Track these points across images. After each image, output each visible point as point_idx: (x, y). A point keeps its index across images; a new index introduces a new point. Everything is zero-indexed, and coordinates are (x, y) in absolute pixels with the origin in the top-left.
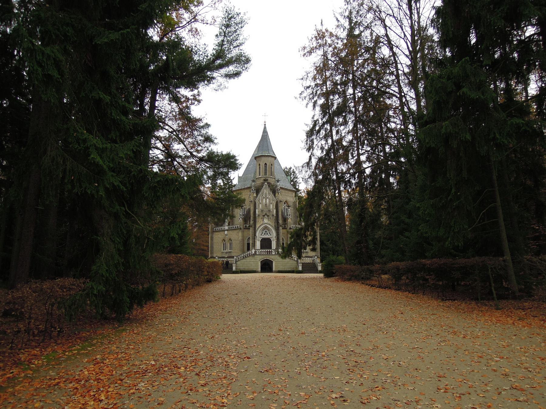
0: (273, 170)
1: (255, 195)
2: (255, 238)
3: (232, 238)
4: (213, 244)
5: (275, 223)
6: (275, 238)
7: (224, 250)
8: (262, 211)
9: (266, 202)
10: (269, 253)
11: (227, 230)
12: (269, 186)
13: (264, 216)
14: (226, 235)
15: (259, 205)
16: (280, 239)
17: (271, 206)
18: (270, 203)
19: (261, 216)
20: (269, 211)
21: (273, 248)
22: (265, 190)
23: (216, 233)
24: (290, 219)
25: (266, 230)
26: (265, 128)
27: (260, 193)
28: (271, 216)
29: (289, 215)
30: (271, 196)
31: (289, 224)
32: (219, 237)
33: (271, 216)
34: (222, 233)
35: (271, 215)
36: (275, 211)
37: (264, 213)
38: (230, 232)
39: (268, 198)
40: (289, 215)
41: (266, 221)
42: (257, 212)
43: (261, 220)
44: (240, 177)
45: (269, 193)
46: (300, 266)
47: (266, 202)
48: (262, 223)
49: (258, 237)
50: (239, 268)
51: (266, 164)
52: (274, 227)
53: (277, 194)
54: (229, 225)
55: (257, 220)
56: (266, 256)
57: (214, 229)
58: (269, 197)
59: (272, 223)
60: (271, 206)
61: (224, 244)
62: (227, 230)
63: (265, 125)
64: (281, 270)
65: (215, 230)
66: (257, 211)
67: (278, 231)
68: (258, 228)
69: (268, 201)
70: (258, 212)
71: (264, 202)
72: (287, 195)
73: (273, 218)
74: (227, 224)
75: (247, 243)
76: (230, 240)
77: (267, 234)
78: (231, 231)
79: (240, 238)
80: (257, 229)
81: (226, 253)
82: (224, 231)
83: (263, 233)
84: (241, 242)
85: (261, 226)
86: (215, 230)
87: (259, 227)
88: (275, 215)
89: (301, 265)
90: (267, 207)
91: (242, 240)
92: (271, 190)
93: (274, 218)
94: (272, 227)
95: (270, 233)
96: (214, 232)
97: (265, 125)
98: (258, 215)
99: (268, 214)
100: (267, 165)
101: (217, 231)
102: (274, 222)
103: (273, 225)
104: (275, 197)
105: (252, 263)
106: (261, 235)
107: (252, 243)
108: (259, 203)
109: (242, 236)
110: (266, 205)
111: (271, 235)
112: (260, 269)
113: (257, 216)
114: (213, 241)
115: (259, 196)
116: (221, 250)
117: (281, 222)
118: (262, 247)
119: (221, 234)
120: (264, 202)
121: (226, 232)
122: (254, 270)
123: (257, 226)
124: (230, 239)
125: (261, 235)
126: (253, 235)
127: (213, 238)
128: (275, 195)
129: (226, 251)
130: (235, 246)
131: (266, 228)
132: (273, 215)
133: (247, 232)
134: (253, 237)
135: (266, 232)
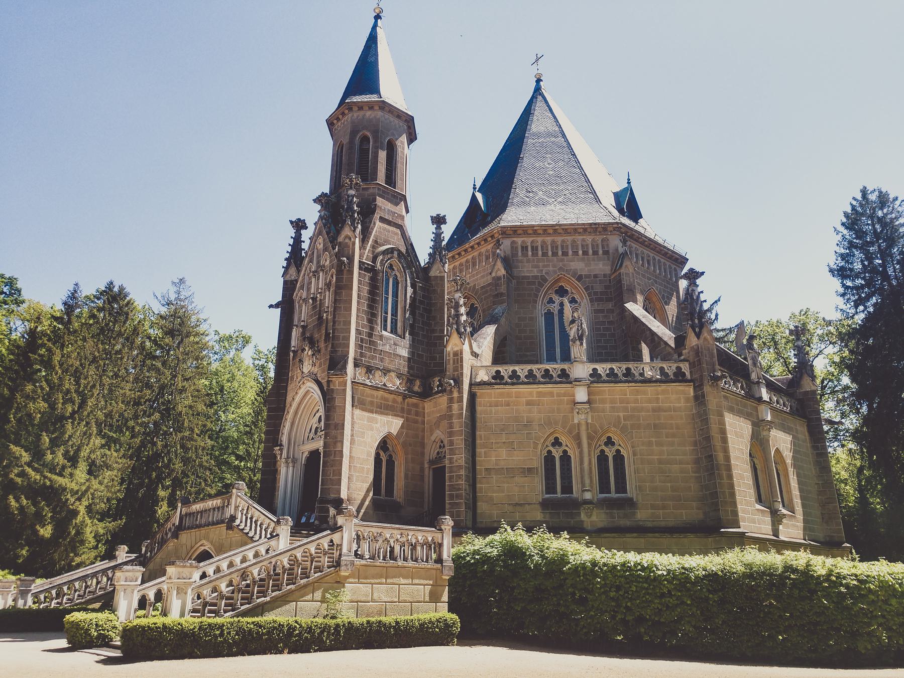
42: (294, 343)
113: (292, 354)
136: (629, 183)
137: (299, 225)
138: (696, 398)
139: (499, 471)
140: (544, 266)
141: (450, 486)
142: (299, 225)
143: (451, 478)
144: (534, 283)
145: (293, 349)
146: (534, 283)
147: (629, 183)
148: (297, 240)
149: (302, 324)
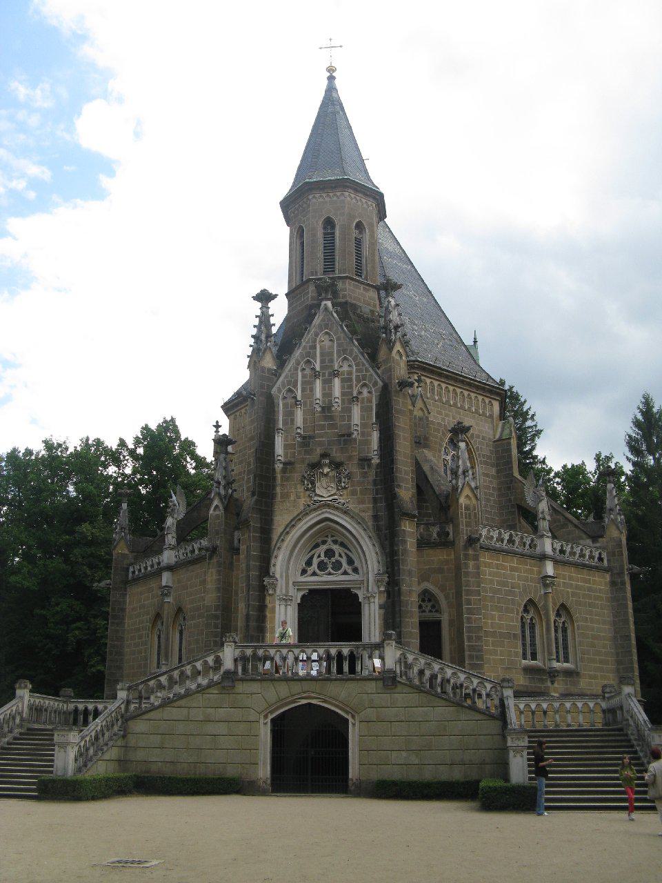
0: (366, 251)
1: (269, 362)
2: (262, 589)
5: (375, 501)
6: (378, 582)
7: (158, 667)
8: (306, 441)
9: (327, 394)
10: (346, 668)
11: (169, 568)
12: (344, 316)
13: (315, 466)
14: (166, 591)
15: (290, 415)
16: (404, 588)
17: (356, 412)
18: (350, 399)
19: (301, 468)
20: (346, 438)
21: (366, 639)
22: (321, 337)
24: (467, 492)
25: (330, 545)
26: (331, 90)
27: (297, 353)
28: (353, 468)
29: (464, 472)
30: (351, 364)
31: (463, 520)
34: (153, 584)
36: (375, 436)
37: (319, 451)
40: (464, 472)
41: (324, 490)
42: (279, 449)
43: (300, 489)
45: (343, 351)
46: (518, 750)
47: (327, 394)
48: (302, 501)
49: (281, 584)
50: (140, 755)
51: (329, 223)
52: (370, 524)
53: (383, 350)
54: (182, 538)
55: (278, 490)
57: (131, 569)
58: (345, 368)
59: (362, 502)
60: (356, 412)
63: (331, 79)
64: (394, 773)
67: (392, 544)
68: (286, 532)
70: (286, 447)
71: (318, 393)
72: (462, 407)
73: (364, 475)
74: (171, 539)
77: (337, 566)
79: (211, 598)
80: (275, 537)
82: (158, 573)
83: (315, 561)
84: (216, 617)
86: (134, 572)
87: (291, 525)
88: (376, 461)
89: (524, 742)
90: (331, 418)
91: (217, 607)
92: (354, 332)
94: (360, 522)
95: (350, 562)
97: (331, 79)
98: (285, 464)
99: (337, 455)
100: (333, 227)
103: (368, 515)
105: (222, 728)
106: (304, 572)
107: (248, 617)
108: (290, 401)
109: (218, 589)
110: (327, 409)
111: (356, 570)
112: (264, 771)
113: (278, 467)
115: (290, 365)
117: (406, 493)
118: (307, 634)
120: (318, 393)
121: (166, 578)
122: (231, 772)
123: (281, 520)
124: (180, 610)
125: (304, 572)
126: (254, 573)
128: (373, 358)
131: (326, 533)
132: (365, 461)
134: (254, 583)
135: (330, 553)
136: (475, 342)
137: (265, 297)
138: (613, 583)
139: (493, 634)
140: (447, 415)
141: (469, 646)
142: (265, 297)
143: (470, 639)
144: (438, 430)
145: (280, 458)
146: (438, 430)
147: (475, 342)
148: (264, 319)
149: (299, 431)
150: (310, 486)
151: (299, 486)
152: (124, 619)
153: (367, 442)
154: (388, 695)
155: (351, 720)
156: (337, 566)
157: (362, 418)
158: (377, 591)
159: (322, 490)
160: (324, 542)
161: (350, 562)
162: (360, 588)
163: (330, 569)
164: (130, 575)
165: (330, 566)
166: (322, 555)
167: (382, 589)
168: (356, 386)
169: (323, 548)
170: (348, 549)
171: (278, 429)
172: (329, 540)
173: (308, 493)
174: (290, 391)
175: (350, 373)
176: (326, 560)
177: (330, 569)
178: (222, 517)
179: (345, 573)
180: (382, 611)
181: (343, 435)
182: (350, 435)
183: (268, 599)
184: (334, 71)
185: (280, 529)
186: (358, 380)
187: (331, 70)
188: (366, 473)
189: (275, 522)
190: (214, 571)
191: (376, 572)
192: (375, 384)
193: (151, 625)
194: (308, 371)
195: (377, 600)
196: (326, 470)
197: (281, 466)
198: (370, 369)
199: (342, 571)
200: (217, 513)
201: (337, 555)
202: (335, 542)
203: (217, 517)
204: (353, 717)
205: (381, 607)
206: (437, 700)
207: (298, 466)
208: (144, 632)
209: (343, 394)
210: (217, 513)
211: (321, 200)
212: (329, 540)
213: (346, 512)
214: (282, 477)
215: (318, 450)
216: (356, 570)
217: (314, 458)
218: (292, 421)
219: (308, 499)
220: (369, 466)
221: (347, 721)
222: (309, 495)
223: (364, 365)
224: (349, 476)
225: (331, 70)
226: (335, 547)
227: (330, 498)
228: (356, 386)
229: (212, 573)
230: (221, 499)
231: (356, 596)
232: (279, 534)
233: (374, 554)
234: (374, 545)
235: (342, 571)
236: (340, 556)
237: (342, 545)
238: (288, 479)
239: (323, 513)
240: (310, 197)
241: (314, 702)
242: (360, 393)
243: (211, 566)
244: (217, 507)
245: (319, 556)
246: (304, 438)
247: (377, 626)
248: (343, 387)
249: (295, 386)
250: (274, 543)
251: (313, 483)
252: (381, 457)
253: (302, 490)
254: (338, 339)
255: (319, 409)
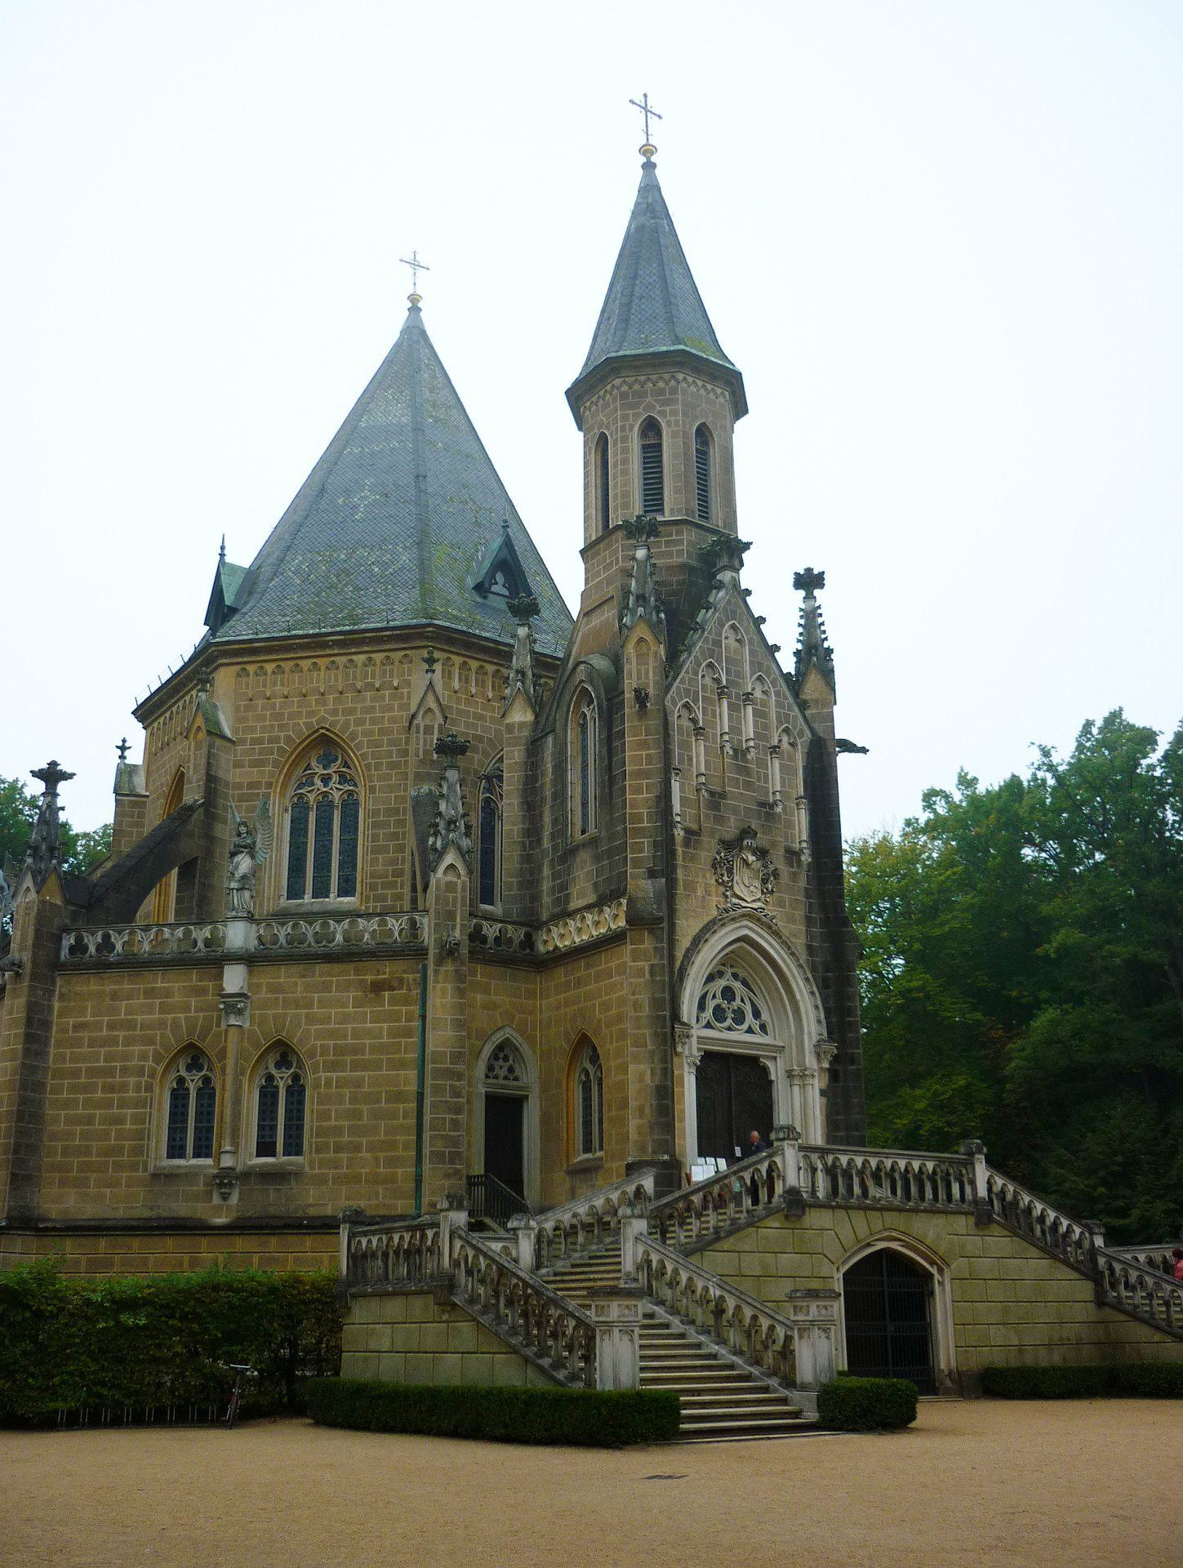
3: (307, 1037)
4: (39, 1087)
5: (809, 921)
7: (176, 1150)
8: (716, 799)
9: (735, 729)
11: (250, 959)
13: (732, 845)
14: (233, 1004)
15: (686, 746)
19: (708, 850)
23: (91, 985)
28: (778, 861)
32: (130, 1025)
33: (778, 861)
35: (782, 852)
36: (801, 820)
38: (270, 976)
39: (748, 697)
41: (747, 890)
42: (677, 807)
44: (234, 569)
48: (715, 900)
55: (680, 873)
56: (891, 1218)
59: (794, 922)
61: (179, 1096)
62: (250, 959)
63: (649, 167)
65: (79, 948)
66: (675, 786)
69: (749, 730)
73: (794, 876)
75: (492, 1101)
76: (284, 1053)
78: (296, 969)
80: (679, 954)
81: (224, 1180)
83: (711, 1005)
85: (709, 929)
86: (79, 948)
87: (698, 941)
88: (806, 858)
90: (746, 771)
93: (802, 882)
95: (757, 1014)
96: (57, 966)
97: (649, 167)
101: (109, 966)
102: (800, 913)
103: (800, 943)
104: (803, 706)
108: (686, 724)
110: (740, 753)
113: (679, 833)
114: (41, 1054)
116: (139, 1151)
119: (150, 993)
121: (234, 979)
123: (687, 929)
127: (46, 1024)
129: (227, 1161)
130: (355, 1115)
132: (792, 855)
133: (486, 992)
135: (728, 993)
150: (726, 878)
151: (708, 875)
152: (47, 1045)
153: (789, 825)
154: (979, 1238)
155: (937, 1276)
156: (739, 1017)
157: (783, 784)
158: (815, 1066)
159: (743, 887)
160: (721, 974)
161: (757, 1014)
162: (775, 1058)
163: (729, 1022)
164: (64, 953)
165: (730, 1015)
166: (719, 995)
167: (826, 1065)
168: (778, 729)
169: (721, 983)
170: (752, 991)
171: (674, 769)
172: (728, 975)
173: (722, 889)
174: (687, 706)
175: (764, 704)
176: (725, 1005)
177: (729, 1022)
178: (463, 889)
179: (750, 1031)
180: (824, 1100)
181: (762, 804)
182: (772, 806)
183: (676, 1060)
184: (652, 154)
185: (688, 945)
186: (780, 722)
187: (647, 150)
188: (794, 873)
189: (678, 929)
190: (449, 986)
191: (815, 1038)
192: (801, 732)
193: (160, 1069)
194: (708, 681)
195: (816, 1082)
196: (751, 858)
197: (682, 833)
198: (796, 708)
199: (745, 1026)
200: (451, 878)
201: (738, 999)
202: (735, 976)
203: (450, 887)
204: (941, 1271)
205: (823, 1093)
206: (1033, 1249)
207: (704, 839)
208: (132, 1080)
209: (758, 736)
210: (451, 878)
211: (693, 388)
212: (728, 975)
213: (776, 934)
214: (684, 852)
215: (732, 817)
216: (763, 1027)
217: (731, 830)
218: (690, 759)
219: (722, 899)
220: (799, 861)
221: (932, 1275)
222: (724, 894)
223: (785, 698)
224: (776, 874)
225: (647, 150)
226: (737, 985)
227: (755, 905)
228: (778, 729)
229: (444, 992)
230: (463, 854)
231: (765, 1071)
232: (683, 951)
233: (810, 1008)
234: (812, 993)
235: (745, 1026)
236: (742, 1001)
237: (745, 983)
238: (693, 858)
239: (740, 927)
240: (680, 376)
241: (894, 1245)
242: (780, 741)
243: (441, 978)
244: (452, 867)
245: (714, 997)
246: (712, 793)
247: (819, 1126)
248: (755, 723)
249: (696, 701)
250: (678, 964)
251: (730, 872)
252: (815, 853)
253: (713, 882)
254: (751, 642)
255: (731, 752)
